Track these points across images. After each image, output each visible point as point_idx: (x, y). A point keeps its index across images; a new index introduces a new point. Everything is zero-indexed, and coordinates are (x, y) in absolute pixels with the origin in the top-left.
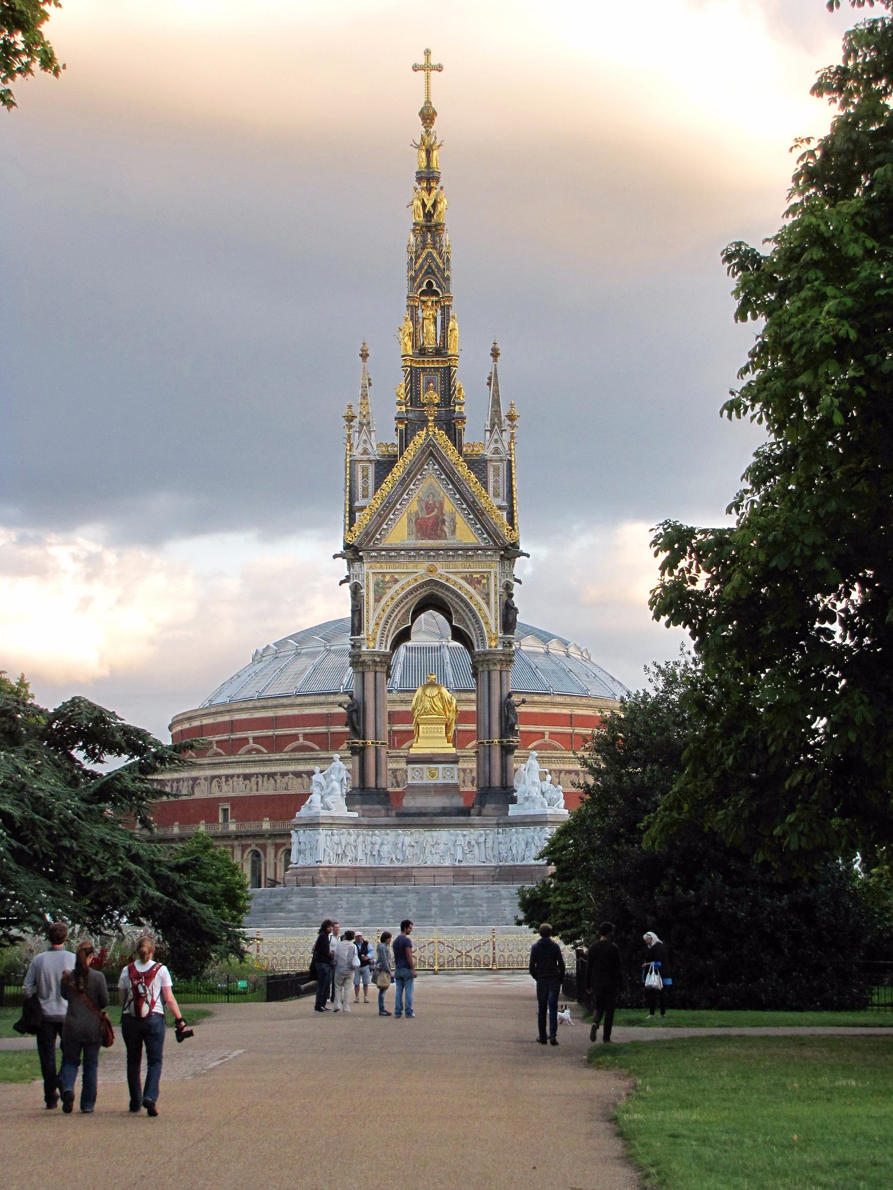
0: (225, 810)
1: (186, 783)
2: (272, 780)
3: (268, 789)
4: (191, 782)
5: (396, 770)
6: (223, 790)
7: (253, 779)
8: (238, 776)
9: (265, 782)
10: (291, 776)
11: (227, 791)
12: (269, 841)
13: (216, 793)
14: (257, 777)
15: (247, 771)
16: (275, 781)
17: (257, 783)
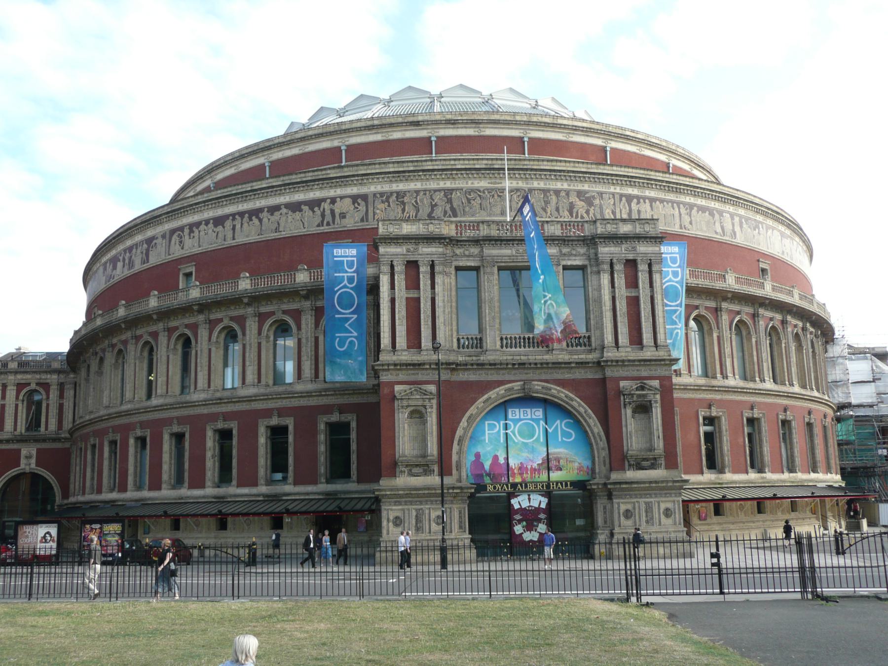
0: (188, 275)
1: (139, 251)
2: (255, 221)
3: (248, 234)
4: (145, 246)
5: (451, 191)
6: (186, 247)
7: (228, 224)
8: (207, 222)
9: (245, 225)
10: (284, 211)
11: (191, 246)
12: (250, 310)
13: (177, 252)
14: (234, 219)
15: (220, 212)
16: (260, 220)
17: (234, 228)
